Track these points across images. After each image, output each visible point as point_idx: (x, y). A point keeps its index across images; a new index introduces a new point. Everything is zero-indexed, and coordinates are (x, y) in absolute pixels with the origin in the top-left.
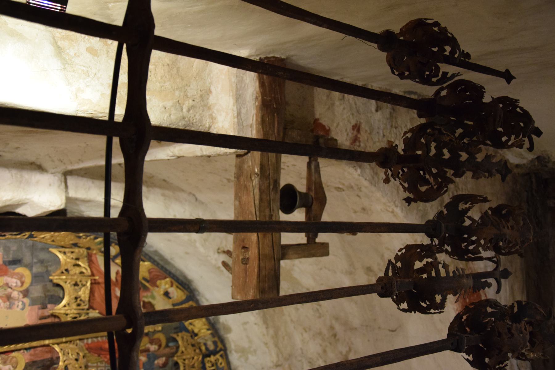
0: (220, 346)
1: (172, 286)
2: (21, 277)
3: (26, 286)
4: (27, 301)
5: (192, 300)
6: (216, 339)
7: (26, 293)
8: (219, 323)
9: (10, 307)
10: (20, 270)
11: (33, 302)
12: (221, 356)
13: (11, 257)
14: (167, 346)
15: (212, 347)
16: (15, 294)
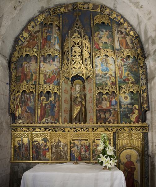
0: (47, 10)
1: (30, 26)
2: (25, 64)
3: (27, 63)
4: (30, 63)
5: (19, 38)
6: (45, 12)
7: (28, 63)
8: (41, 11)
9: (31, 66)
10: (23, 64)
11: (31, 61)
12: (50, 10)
13: (20, 66)
14: (46, 27)
15: (48, 13)
16: (28, 65)
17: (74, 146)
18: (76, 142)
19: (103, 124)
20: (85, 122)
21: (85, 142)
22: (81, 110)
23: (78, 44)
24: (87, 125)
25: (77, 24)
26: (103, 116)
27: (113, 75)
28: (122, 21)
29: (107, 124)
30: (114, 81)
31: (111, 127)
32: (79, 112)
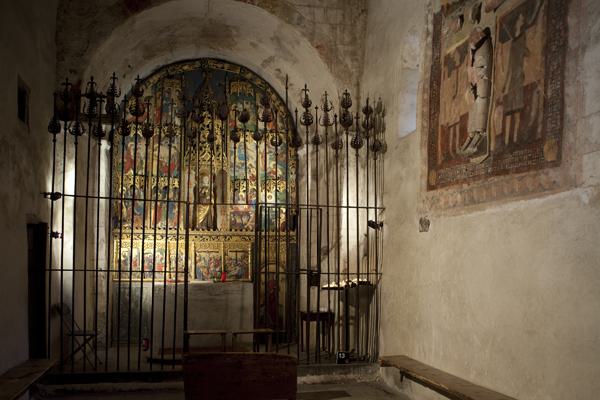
17: (200, 260)
18: (203, 255)
19: (239, 232)
20: (215, 228)
21: (215, 254)
22: (210, 210)
23: (208, 126)
24: (216, 233)
25: (206, 93)
26: (238, 221)
27: (254, 165)
28: (269, 90)
29: (244, 232)
30: (255, 174)
31: (248, 236)
32: (207, 216)
